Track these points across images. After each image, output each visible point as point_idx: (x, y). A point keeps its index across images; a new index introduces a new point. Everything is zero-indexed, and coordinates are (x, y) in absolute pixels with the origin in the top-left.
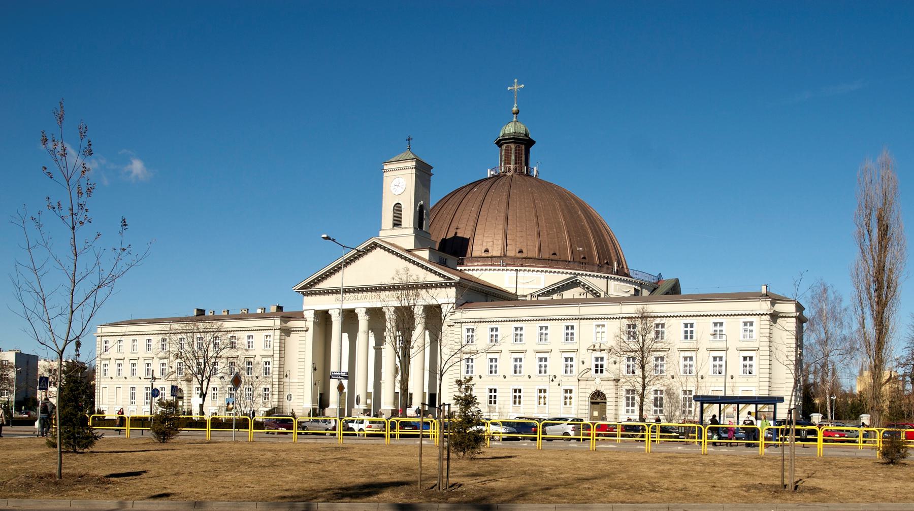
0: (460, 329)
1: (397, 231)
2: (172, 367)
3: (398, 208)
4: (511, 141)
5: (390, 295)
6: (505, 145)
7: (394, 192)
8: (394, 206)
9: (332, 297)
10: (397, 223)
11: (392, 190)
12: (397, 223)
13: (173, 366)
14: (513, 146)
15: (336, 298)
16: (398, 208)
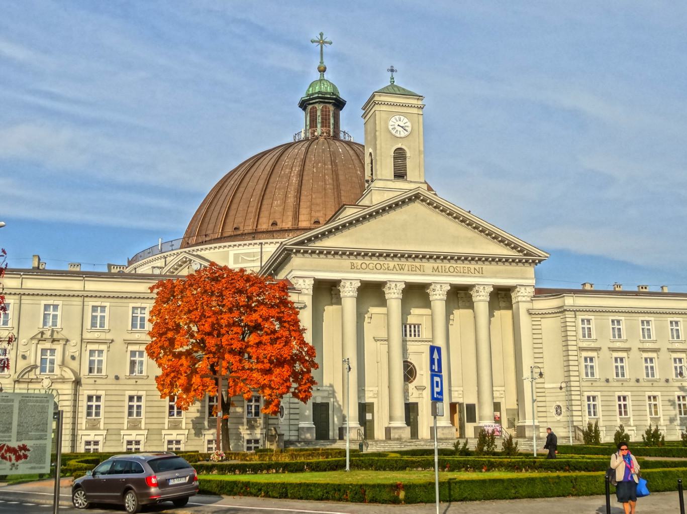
0: (573, 320)
1: (401, 185)
2: (24, 357)
3: (400, 155)
4: (331, 101)
5: (440, 268)
6: (310, 107)
7: (390, 128)
8: (395, 150)
9: (346, 262)
10: (400, 175)
11: (391, 129)
12: (400, 175)
13: (27, 354)
14: (319, 107)
15: (352, 264)
16: (400, 155)
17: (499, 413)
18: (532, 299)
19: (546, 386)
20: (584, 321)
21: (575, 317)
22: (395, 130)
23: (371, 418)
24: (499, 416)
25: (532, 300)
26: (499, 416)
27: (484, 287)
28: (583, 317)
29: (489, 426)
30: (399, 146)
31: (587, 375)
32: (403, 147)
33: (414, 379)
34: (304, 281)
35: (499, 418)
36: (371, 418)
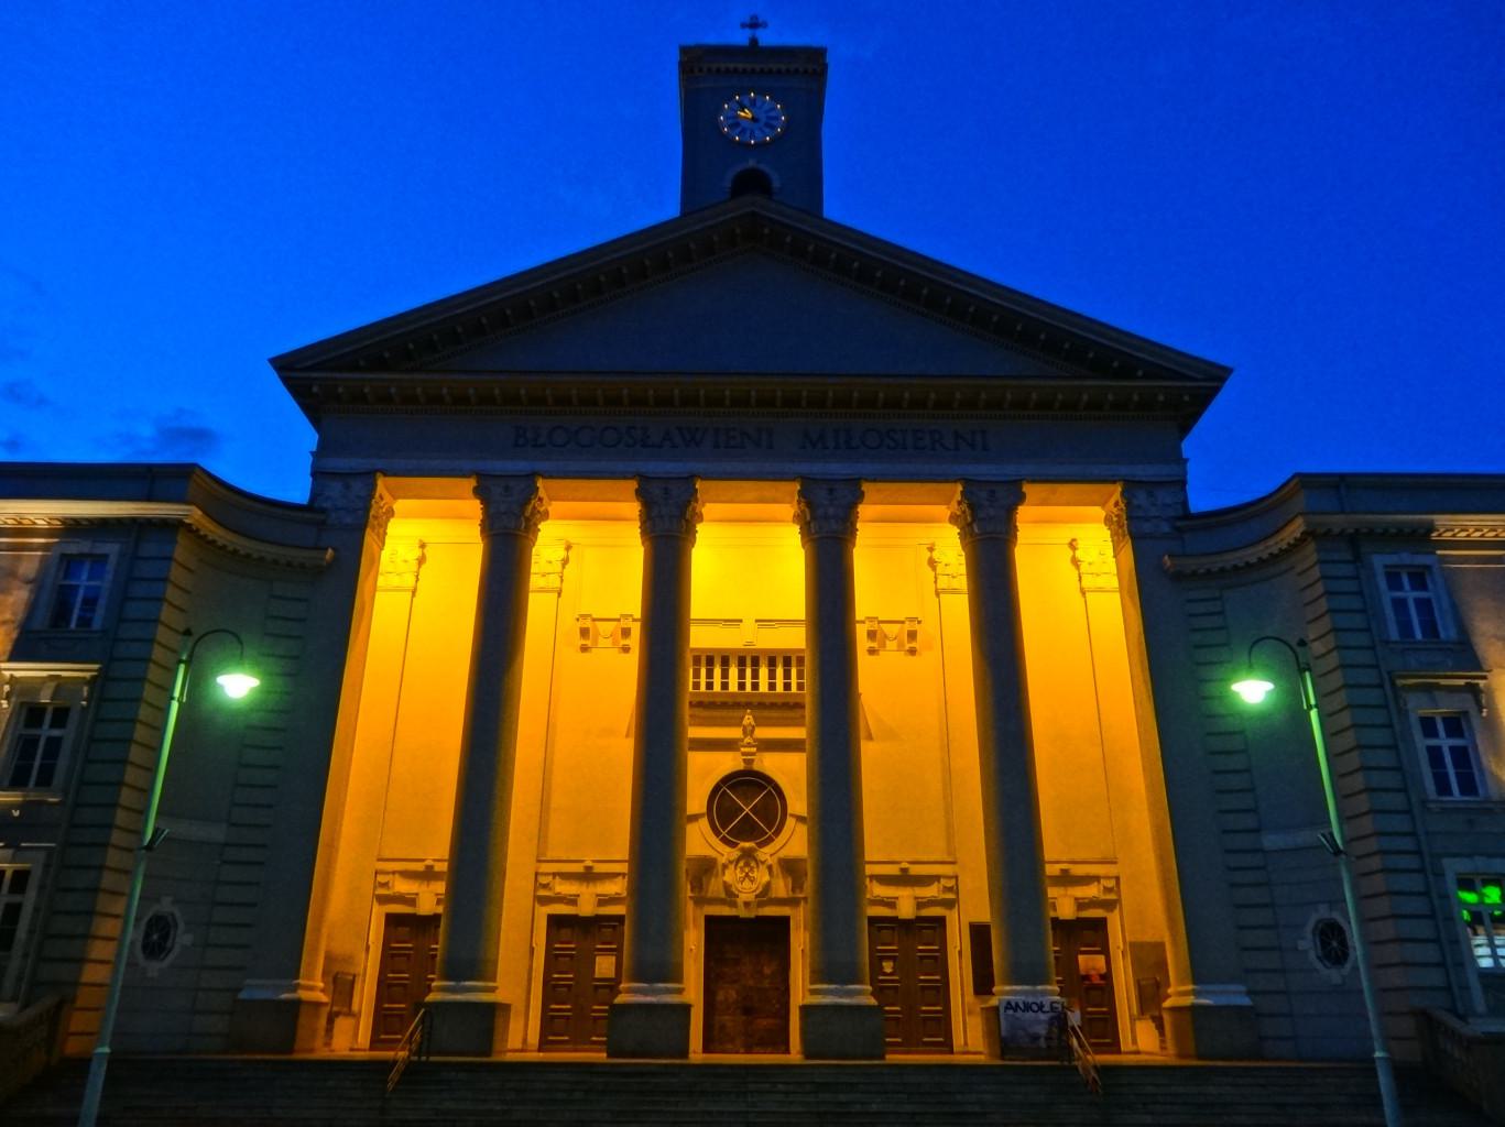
17: (1101, 958)
18: (1179, 524)
19: (1271, 841)
20: (1398, 575)
21: (1357, 559)
22: (739, 129)
23: (611, 974)
24: (1104, 970)
25: (1178, 529)
26: (1104, 970)
27: (992, 492)
28: (1393, 559)
29: (1028, 1007)
30: (751, 163)
31: (1443, 787)
32: (762, 167)
33: (778, 832)
34: (347, 487)
35: (1103, 977)
36: (611, 974)
